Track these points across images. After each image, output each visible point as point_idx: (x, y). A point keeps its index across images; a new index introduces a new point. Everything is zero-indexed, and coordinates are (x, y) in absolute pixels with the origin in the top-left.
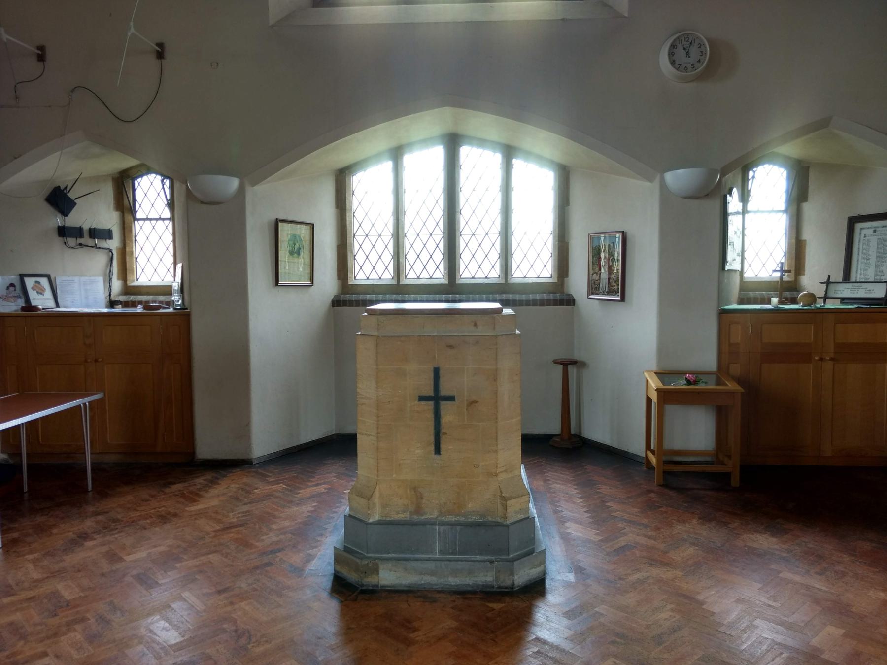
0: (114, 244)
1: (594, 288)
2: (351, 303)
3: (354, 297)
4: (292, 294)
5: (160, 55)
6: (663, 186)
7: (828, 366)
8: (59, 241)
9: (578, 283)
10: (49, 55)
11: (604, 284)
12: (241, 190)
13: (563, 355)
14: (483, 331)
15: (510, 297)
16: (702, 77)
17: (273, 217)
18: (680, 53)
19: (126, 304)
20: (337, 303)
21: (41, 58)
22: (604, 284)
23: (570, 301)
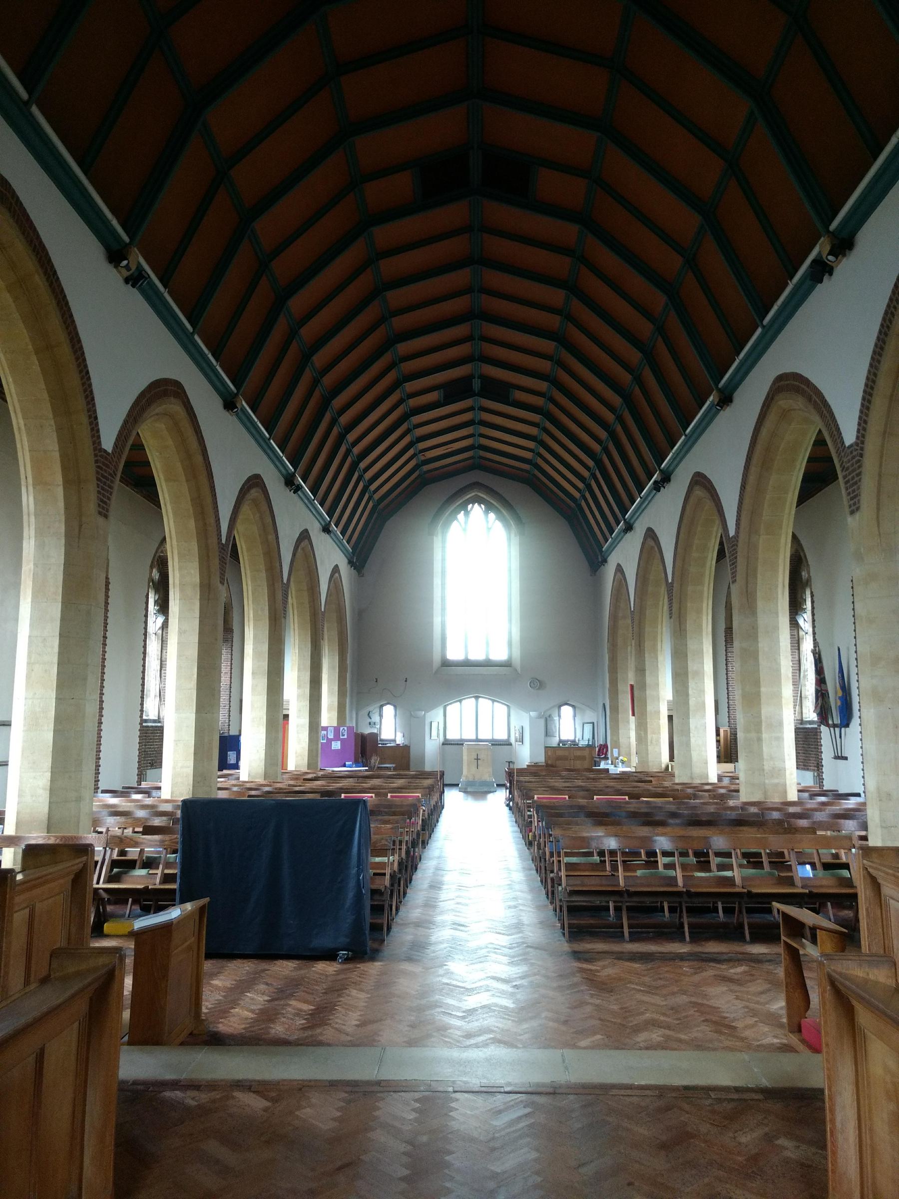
0: (378, 727)
1: (516, 741)
2: (446, 744)
3: (448, 742)
4: (433, 742)
5: (406, 681)
6: (530, 716)
7: (572, 761)
8: (368, 725)
9: (513, 740)
10: (378, 679)
11: (518, 740)
12: (425, 714)
13: (509, 760)
14: (485, 747)
15: (494, 743)
16: (539, 689)
17: (430, 721)
18: (532, 684)
19: (382, 744)
20: (443, 744)
21: (376, 681)
22: (518, 740)
23: (511, 744)
